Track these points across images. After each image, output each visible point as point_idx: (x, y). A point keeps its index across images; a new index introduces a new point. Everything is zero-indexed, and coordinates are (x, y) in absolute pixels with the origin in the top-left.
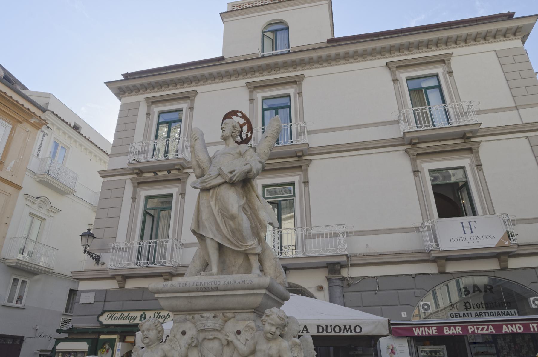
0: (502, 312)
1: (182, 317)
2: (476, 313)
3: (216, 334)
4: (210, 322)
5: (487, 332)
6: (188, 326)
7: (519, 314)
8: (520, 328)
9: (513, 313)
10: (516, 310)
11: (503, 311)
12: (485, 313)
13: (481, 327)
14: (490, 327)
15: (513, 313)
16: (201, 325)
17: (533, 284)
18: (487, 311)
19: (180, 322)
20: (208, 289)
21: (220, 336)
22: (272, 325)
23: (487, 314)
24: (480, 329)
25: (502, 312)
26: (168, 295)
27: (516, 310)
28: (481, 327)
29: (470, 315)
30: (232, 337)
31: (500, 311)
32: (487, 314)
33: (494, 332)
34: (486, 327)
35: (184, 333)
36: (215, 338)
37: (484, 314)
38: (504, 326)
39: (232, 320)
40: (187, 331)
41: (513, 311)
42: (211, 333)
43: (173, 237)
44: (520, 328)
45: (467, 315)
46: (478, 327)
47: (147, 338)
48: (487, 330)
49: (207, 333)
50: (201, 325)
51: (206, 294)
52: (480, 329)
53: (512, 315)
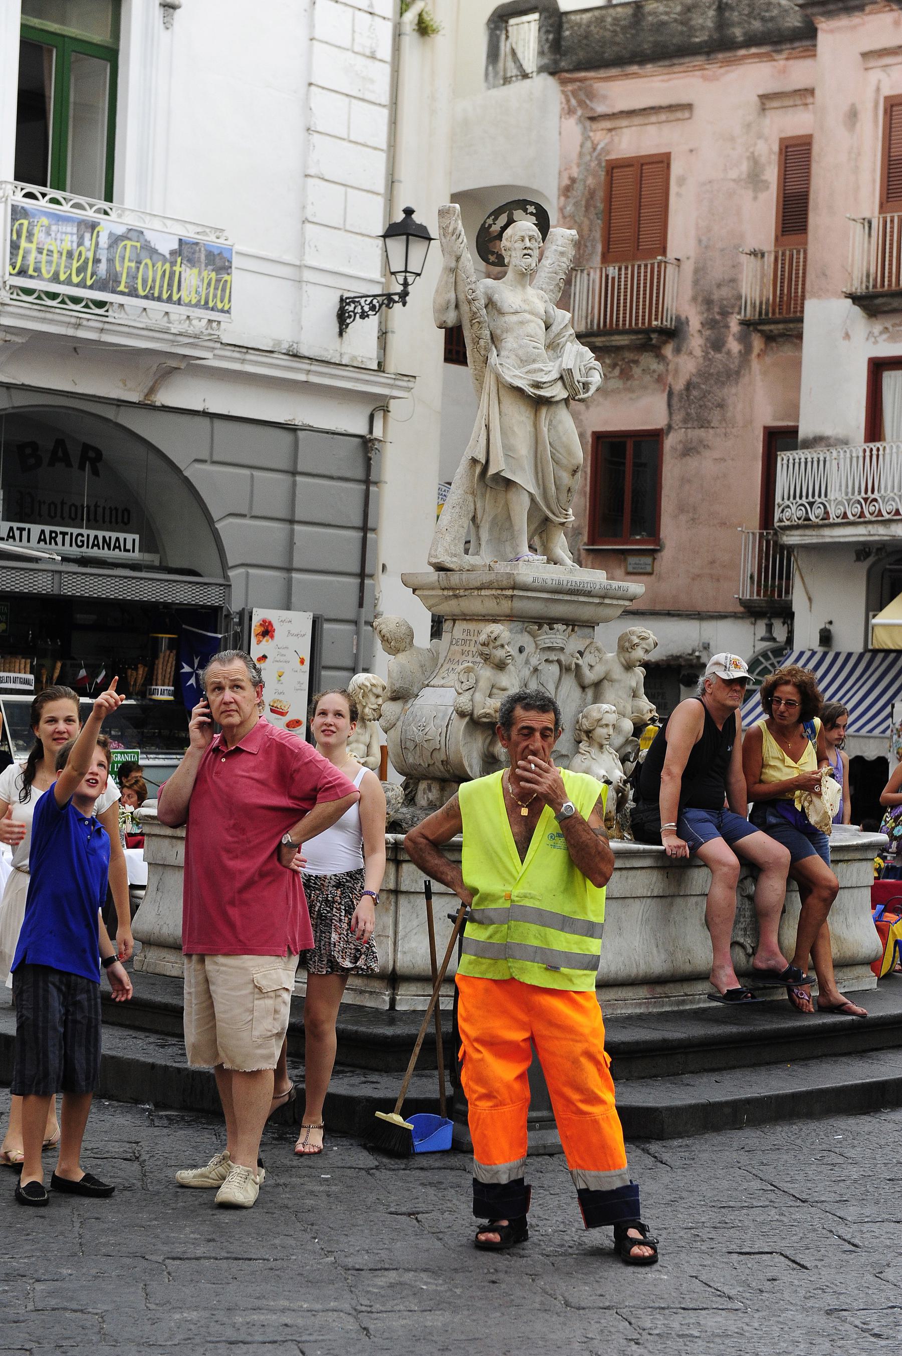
0: (104, 537)
2: (43, 532)
6: (525, 640)
9: (129, 546)
10: (137, 537)
11: (107, 534)
12: (64, 534)
15: (129, 546)
16: (547, 641)
17: (198, 466)
21: (562, 658)
23: (67, 538)
26: (529, 594)
27: (137, 537)
29: (25, 534)
31: (100, 534)
32: (67, 538)
37: (59, 539)
41: (130, 537)
45: (17, 533)
50: (547, 641)
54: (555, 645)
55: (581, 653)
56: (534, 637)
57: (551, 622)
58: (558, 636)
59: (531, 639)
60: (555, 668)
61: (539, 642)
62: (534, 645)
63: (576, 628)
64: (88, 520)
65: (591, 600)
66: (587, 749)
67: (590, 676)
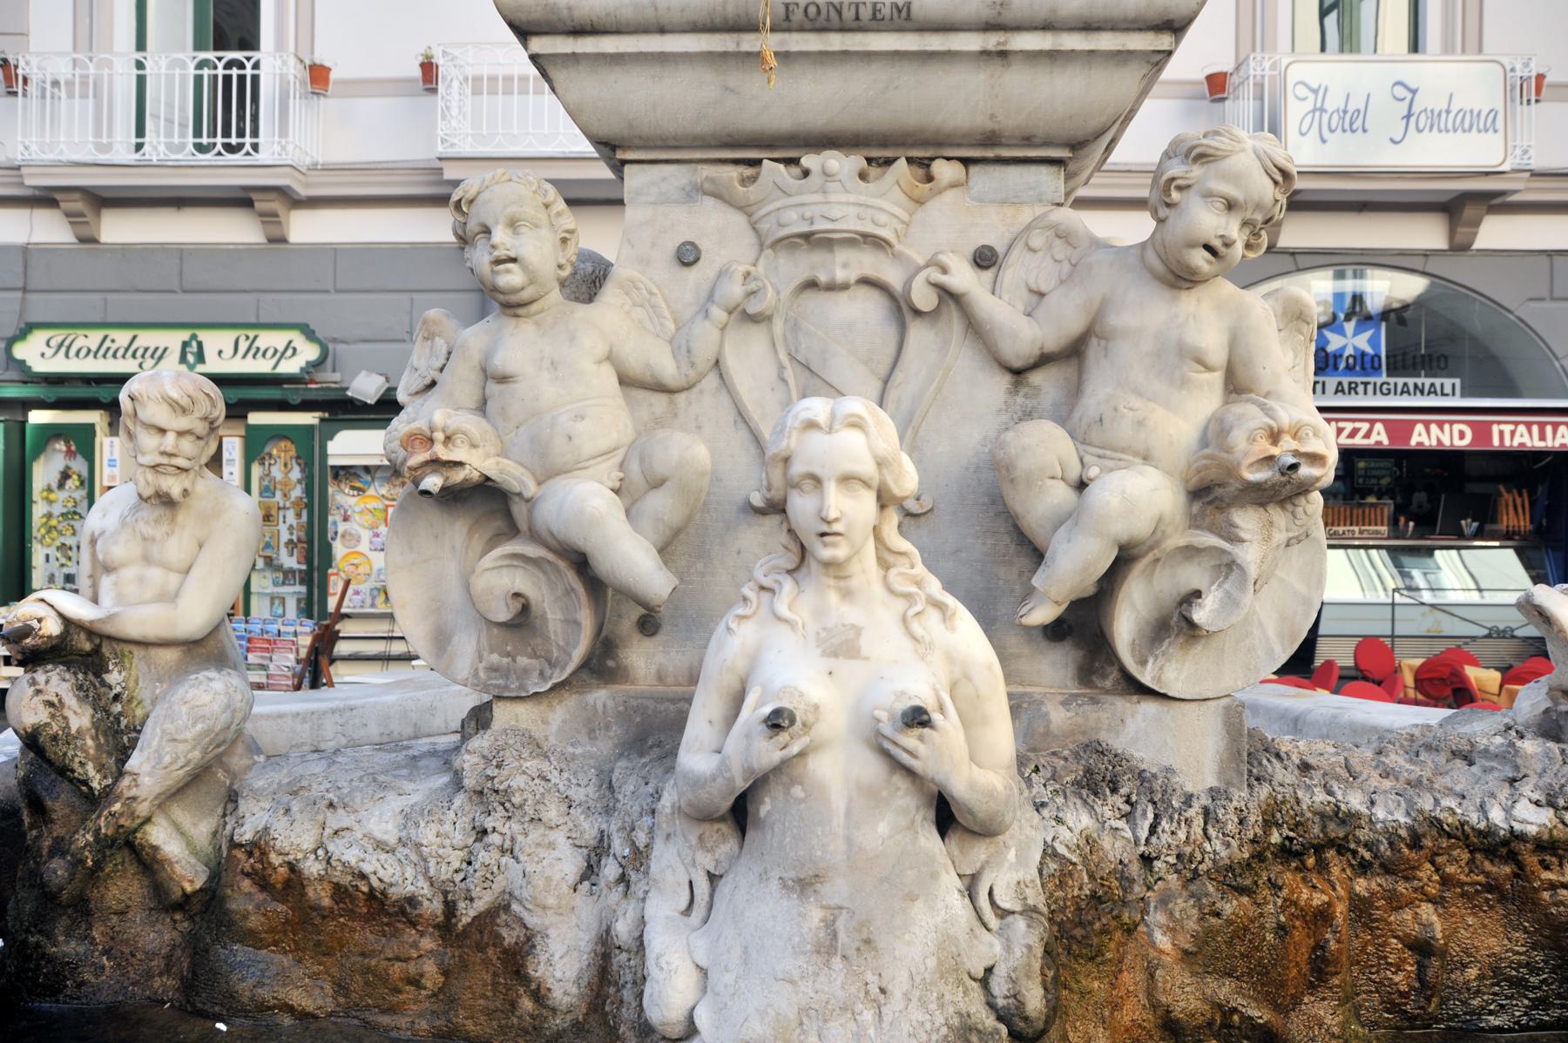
0: (1416, 386)
1: (674, 177)
2: (1340, 383)
3: (866, 262)
4: (843, 198)
5: (1366, 442)
7: (1463, 395)
8: (1462, 435)
9: (1448, 389)
10: (1457, 381)
11: (1419, 381)
12: (1366, 384)
13: (1349, 426)
14: (1379, 427)
15: (1448, 389)
18: (1371, 379)
19: (663, 200)
20: (848, 14)
22: (1231, 206)
23: (1370, 388)
24: (1346, 433)
25: (1416, 386)
26: (609, 45)
27: (1457, 381)
28: (1349, 426)
30: (963, 277)
31: (1411, 381)
32: (1370, 388)
33: (1386, 442)
34: (1365, 427)
35: (687, 257)
36: (865, 281)
37: (1361, 389)
38: (1419, 428)
39: (949, 196)
40: (704, 245)
41: (1448, 382)
42: (842, 255)
43: (280, 45)
44: (1462, 435)
46: (1341, 424)
47: (514, 260)
48: (1367, 435)
49: (818, 257)
51: (836, 42)
52: (1346, 433)
53: (1443, 394)
54: (818, 226)
55: (984, 259)
56: (744, 208)
57: (793, 146)
58: (839, 192)
59: (737, 220)
60: (865, 310)
61: (764, 226)
62: (749, 238)
63: (945, 171)
64: (1388, 369)
65: (934, 42)
66: (767, 582)
67: (1024, 334)
